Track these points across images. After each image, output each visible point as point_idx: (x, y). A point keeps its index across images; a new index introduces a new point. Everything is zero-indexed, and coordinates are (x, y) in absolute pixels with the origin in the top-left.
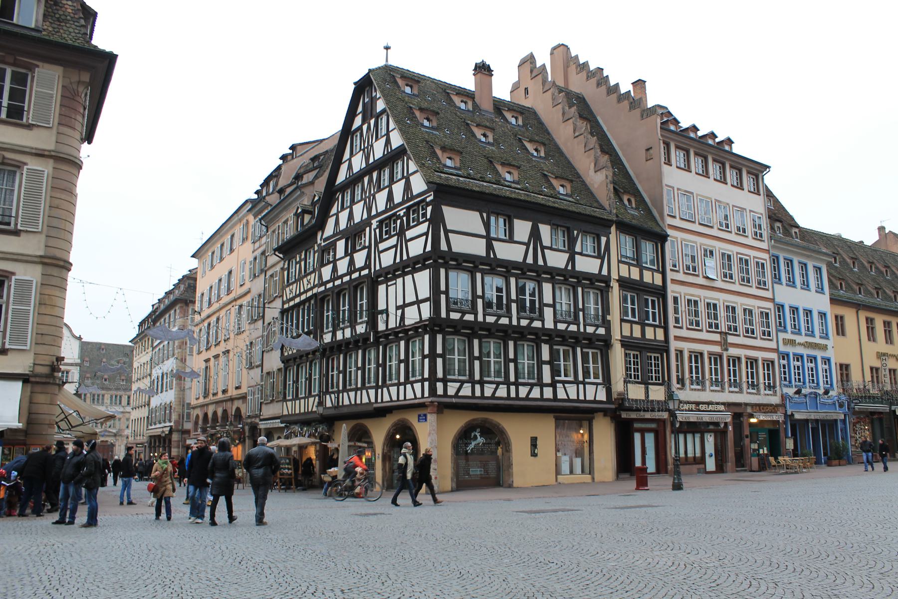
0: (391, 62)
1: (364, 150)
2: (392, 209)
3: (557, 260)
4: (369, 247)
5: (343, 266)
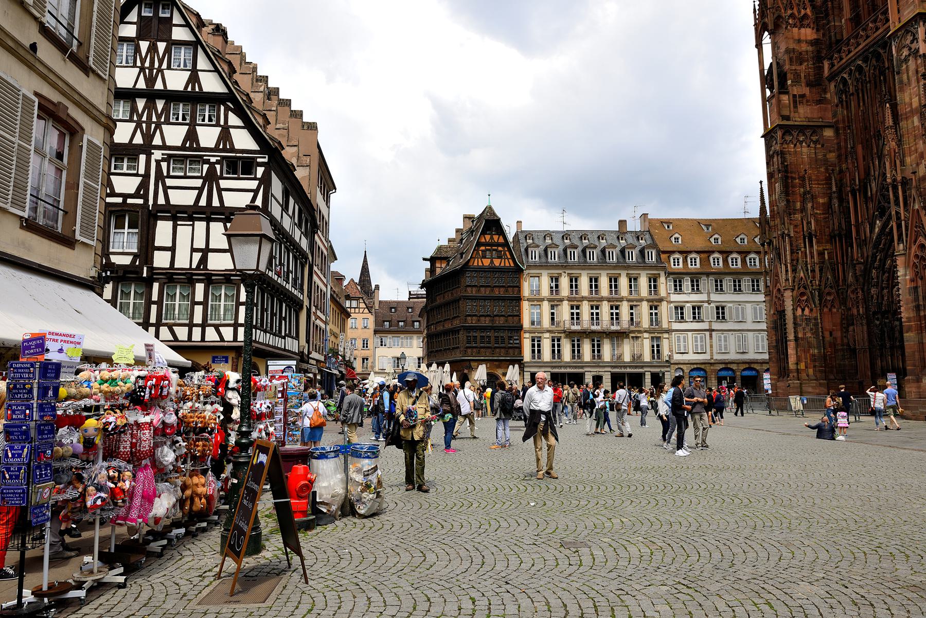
1: (142, 69)
2: (191, 149)
3: (297, 234)
4: (146, 176)
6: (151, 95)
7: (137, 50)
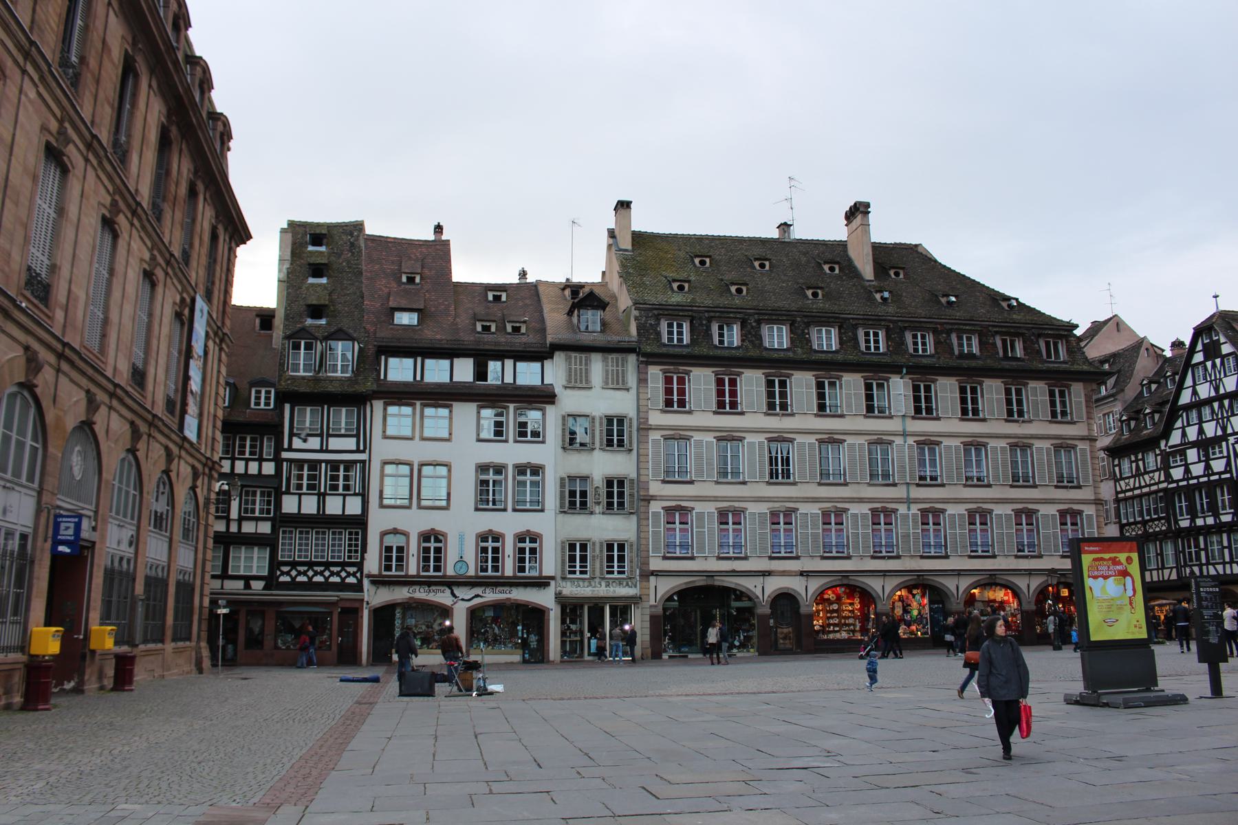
0: (1221, 308)
1: (1211, 382)
4: (1228, 457)
5: (1198, 470)
6: (1220, 398)
7: (1206, 369)
